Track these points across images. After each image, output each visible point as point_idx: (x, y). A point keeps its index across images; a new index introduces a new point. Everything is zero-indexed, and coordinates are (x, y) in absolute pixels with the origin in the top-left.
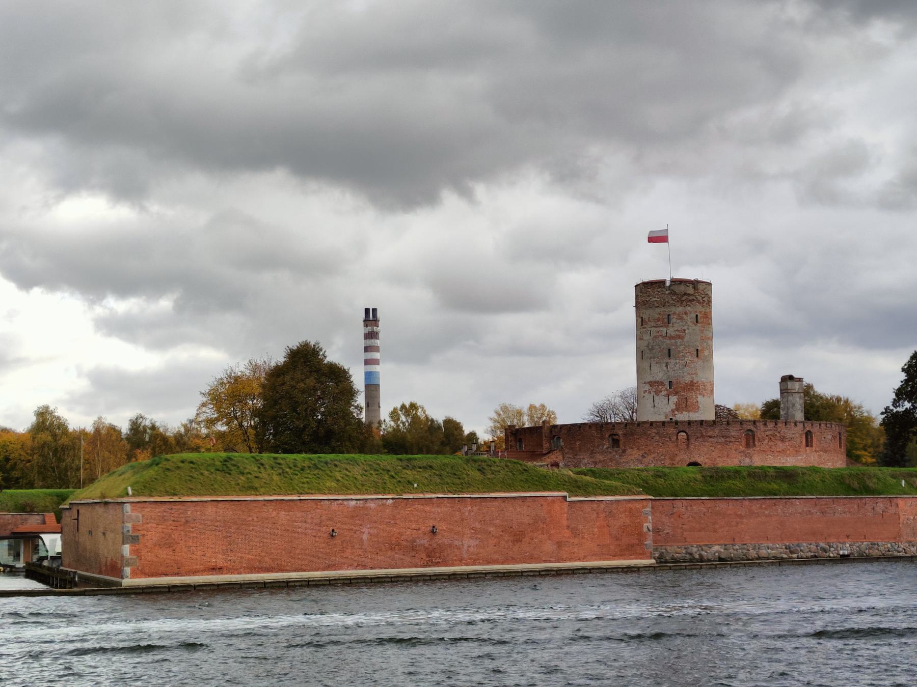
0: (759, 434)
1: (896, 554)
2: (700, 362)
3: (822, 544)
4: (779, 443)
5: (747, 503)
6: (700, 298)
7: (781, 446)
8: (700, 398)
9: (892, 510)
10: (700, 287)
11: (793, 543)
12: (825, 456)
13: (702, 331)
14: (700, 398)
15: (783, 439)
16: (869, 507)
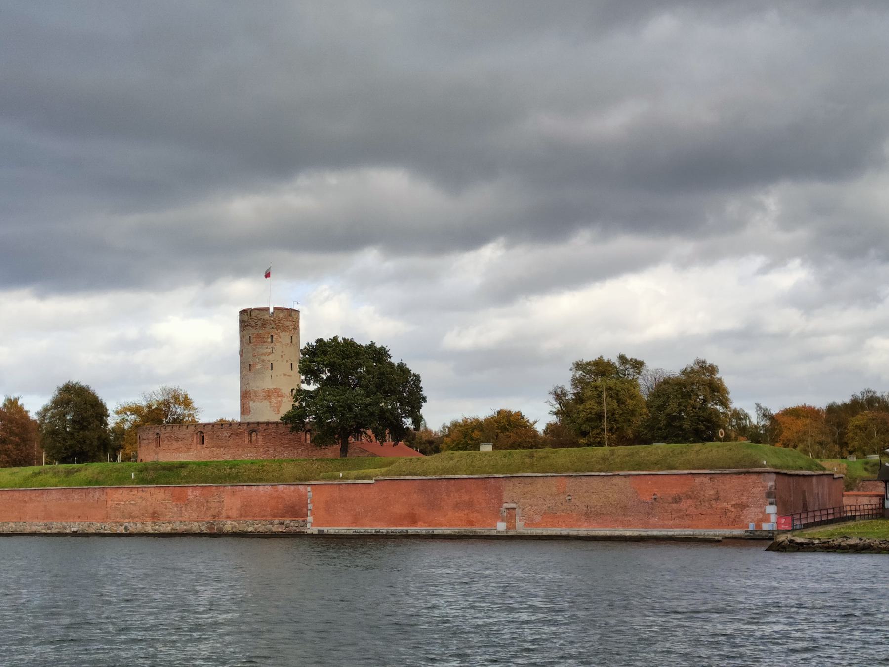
0: (162, 436)
1: (102, 531)
2: (252, 374)
3: (64, 523)
4: (174, 442)
5: (29, 492)
6: (253, 324)
7: (176, 445)
8: (252, 404)
9: (103, 497)
10: (253, 314)
11: (48, 522)
12: (218, 451)
13: (254, 350)
14: (252, 404)
15: (177, 440)
16: (91, 495)
